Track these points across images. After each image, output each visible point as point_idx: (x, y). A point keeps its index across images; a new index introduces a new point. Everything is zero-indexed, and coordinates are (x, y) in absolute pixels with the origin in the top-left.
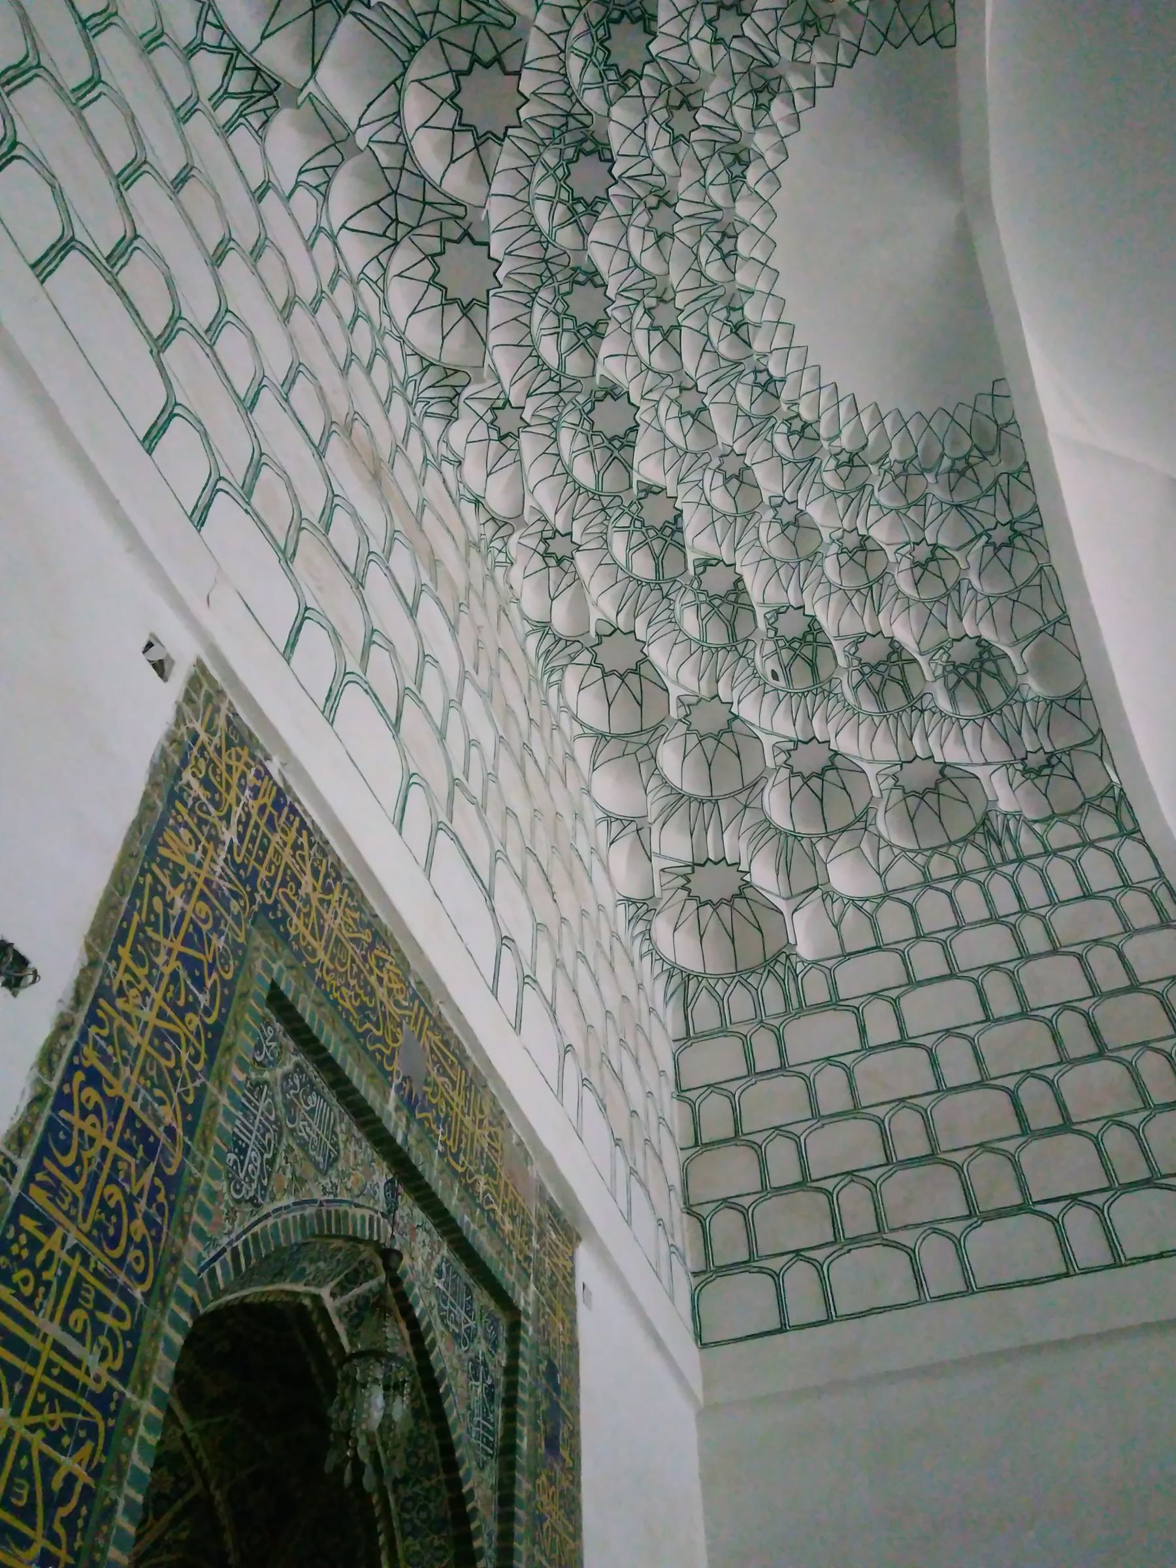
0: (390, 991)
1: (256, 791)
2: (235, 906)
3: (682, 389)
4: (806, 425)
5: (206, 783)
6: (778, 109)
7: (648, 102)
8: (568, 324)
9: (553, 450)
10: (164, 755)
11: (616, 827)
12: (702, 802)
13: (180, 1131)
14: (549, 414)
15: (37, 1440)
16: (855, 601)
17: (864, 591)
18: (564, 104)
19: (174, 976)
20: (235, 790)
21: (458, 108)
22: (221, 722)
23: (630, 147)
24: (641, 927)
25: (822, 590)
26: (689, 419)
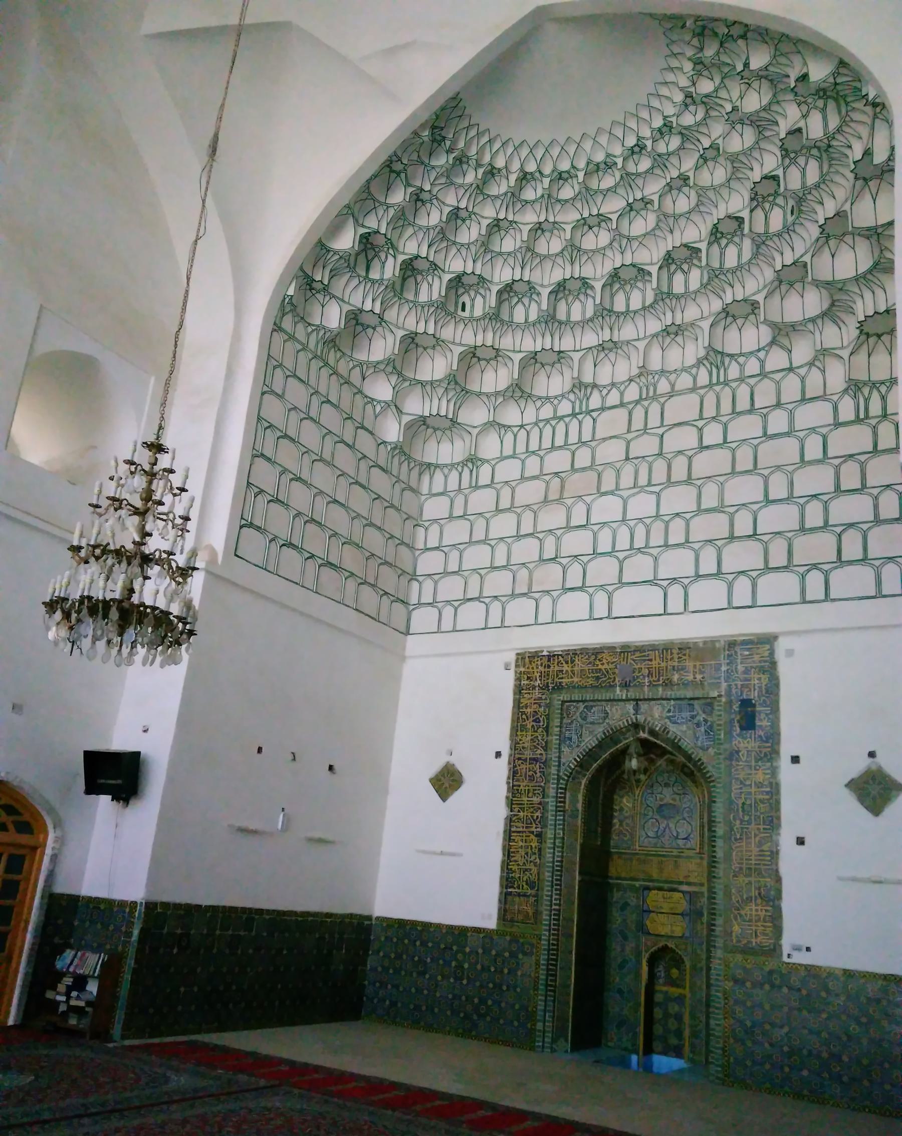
0: (608, 663)
1: (542, 665)
2: (544, 697)
3: (631, 210)
4: (665, 125)
5: (528, 678)
6: (500, 163)
7: (494, 254)
8: (583, 290)
9: (632, 315)
10: (515, 685)
11: (817, 363)
12: (833, 304)
13: (543, 752)
14: (614, 318)
15: (529, 814)
16: (767, 133)
17: (761, 129)
18: (487, 320)
19: (533, 726)
20: (535, 670)
21: (491, 359)
22: (527, 660)
23: (511, 260)
24: (866, 391)
25: (756, 154)
26: (649, 206)
